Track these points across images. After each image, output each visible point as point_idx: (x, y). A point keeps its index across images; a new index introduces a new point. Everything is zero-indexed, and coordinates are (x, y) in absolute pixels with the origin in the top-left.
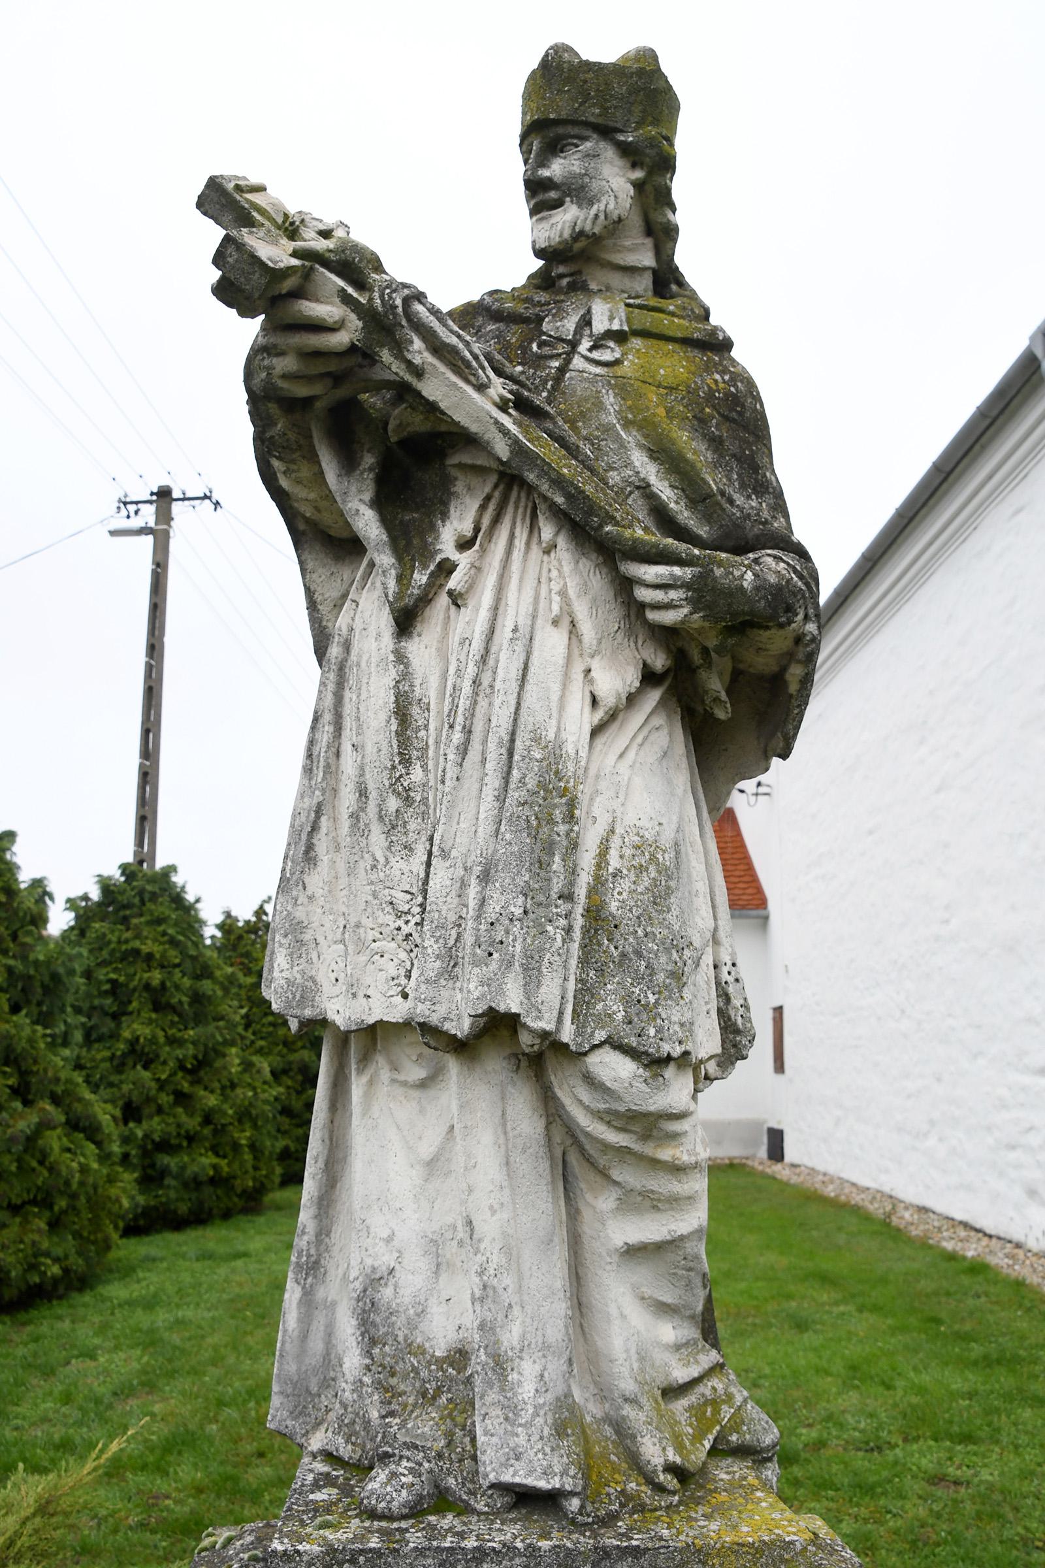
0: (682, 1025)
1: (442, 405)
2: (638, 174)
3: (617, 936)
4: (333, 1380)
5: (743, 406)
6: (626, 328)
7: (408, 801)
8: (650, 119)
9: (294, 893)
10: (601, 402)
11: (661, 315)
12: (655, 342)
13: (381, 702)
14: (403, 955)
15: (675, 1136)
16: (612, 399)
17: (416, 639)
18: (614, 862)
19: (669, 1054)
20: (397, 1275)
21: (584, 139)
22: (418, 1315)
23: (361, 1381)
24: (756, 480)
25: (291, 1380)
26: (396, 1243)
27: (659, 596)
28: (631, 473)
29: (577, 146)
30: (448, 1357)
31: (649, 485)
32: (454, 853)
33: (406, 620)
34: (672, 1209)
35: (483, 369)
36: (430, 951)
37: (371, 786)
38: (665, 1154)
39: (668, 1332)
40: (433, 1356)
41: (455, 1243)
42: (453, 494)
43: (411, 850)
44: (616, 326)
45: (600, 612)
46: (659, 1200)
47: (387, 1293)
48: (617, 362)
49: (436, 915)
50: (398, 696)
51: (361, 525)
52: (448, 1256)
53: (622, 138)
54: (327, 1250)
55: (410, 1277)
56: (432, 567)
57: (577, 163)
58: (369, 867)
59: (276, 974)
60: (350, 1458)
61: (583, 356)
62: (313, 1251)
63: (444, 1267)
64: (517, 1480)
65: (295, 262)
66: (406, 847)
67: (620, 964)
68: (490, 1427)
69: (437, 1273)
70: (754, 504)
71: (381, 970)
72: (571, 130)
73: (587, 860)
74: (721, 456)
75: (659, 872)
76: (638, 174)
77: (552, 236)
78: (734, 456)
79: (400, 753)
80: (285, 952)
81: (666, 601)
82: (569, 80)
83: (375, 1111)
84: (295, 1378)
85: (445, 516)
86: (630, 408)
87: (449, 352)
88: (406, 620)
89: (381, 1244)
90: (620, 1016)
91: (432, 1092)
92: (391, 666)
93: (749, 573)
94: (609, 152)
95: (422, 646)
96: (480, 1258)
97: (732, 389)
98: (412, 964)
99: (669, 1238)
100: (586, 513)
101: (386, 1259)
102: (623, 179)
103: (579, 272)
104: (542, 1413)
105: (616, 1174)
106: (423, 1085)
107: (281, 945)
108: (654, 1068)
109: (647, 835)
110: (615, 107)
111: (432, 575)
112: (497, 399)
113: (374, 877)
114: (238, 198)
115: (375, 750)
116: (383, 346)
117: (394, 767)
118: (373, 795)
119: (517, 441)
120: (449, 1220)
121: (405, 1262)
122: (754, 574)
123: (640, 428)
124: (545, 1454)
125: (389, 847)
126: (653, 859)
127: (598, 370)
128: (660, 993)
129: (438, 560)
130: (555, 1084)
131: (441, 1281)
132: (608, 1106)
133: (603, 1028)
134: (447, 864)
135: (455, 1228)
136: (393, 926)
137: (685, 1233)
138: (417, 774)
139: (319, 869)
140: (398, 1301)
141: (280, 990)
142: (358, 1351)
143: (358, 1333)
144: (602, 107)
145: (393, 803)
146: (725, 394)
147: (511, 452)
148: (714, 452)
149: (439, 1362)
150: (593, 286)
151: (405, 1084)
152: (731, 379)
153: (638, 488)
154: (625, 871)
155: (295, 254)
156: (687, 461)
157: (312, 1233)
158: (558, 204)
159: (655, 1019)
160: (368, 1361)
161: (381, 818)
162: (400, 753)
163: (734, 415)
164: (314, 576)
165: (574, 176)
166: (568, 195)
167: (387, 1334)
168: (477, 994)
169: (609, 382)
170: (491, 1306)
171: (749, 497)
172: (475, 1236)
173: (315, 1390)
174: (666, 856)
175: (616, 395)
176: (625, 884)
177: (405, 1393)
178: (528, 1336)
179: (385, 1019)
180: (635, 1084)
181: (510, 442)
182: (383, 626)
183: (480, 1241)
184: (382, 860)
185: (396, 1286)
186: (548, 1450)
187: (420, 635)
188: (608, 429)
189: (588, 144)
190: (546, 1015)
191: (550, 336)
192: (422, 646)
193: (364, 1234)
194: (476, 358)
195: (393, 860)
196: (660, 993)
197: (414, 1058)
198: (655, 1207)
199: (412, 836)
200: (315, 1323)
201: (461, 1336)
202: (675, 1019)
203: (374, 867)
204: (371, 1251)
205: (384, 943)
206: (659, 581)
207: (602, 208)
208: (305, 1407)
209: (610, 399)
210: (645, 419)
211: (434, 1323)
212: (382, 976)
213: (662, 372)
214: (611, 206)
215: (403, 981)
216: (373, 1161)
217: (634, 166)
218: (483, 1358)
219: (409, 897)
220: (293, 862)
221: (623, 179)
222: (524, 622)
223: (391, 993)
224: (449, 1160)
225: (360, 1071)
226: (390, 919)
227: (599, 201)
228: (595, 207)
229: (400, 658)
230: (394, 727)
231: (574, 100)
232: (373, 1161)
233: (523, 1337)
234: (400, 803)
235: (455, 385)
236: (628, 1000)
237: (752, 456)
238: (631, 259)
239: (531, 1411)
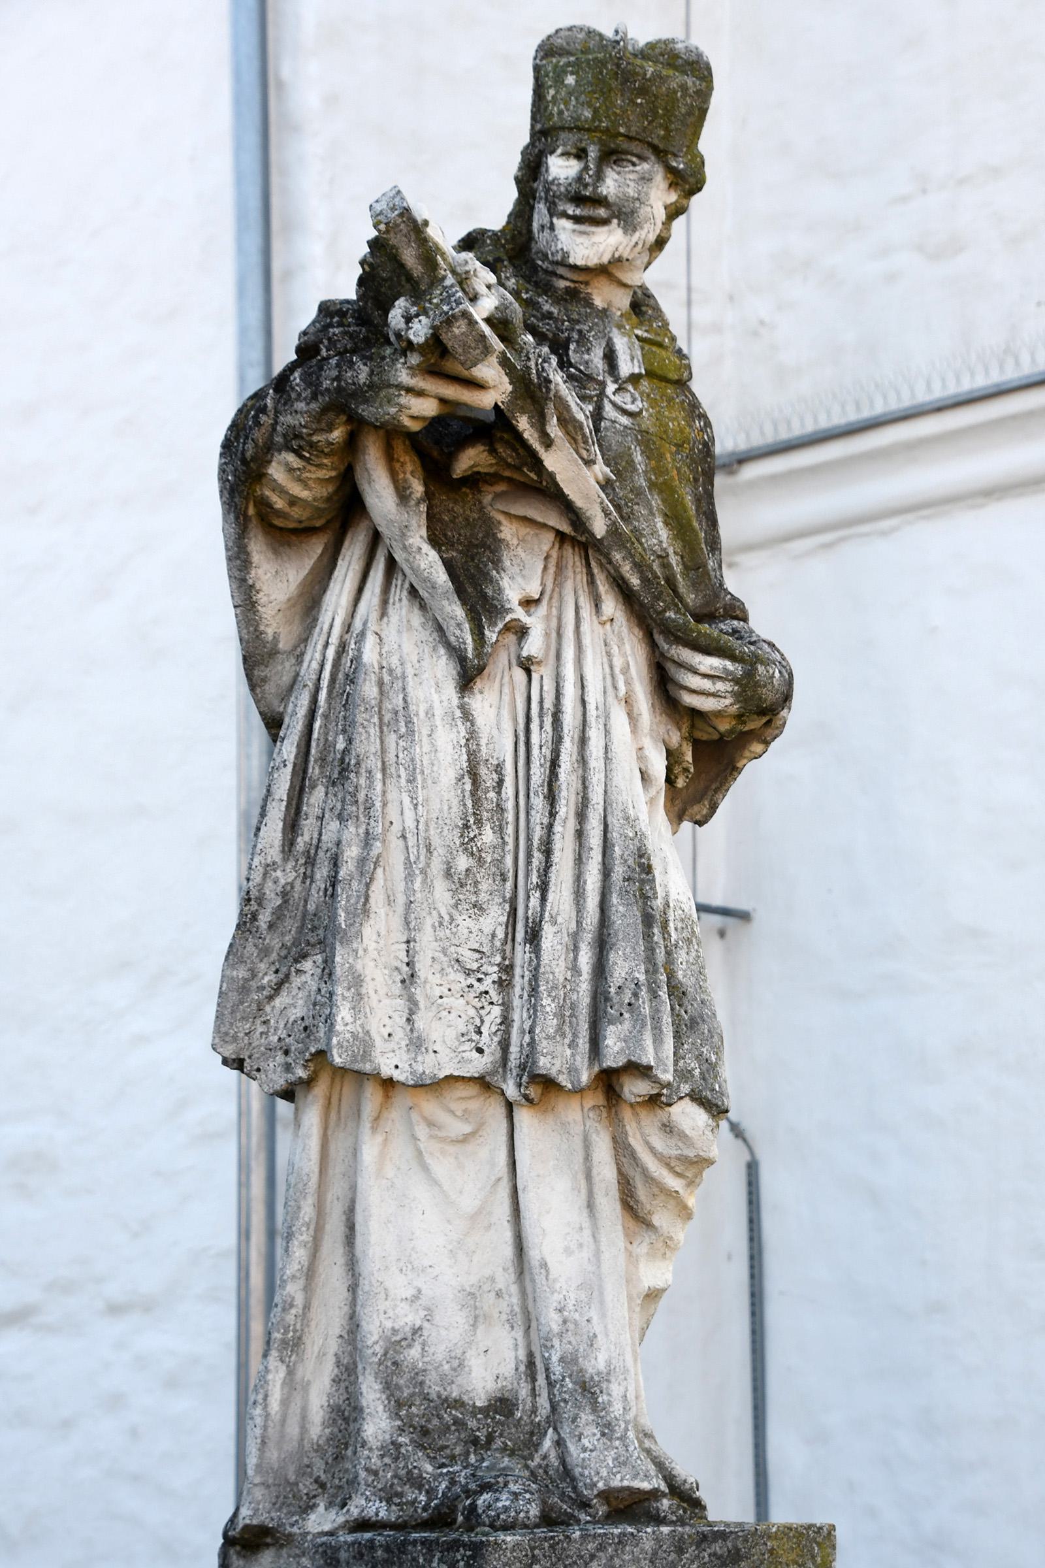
1: (558, 478)
3: (685, 1001)
4: (308, 1466)
7: (480, 861)
9: (355, 945)
10: (633, 461)
13: (449, 759)
14: (472, 1012)
16: (639, 457)
17: (479, 696)
20: (425, 1333)
21: (642, 158)
22: (455, 1370)
23: (397, 1445)
25: (272, 1469)
26: (423, 1301)
27: (706, 684)
28: (655, 541)
29: (634, 164)
30: (489, 1406)
32: (560, 920)
33: (468, 676)
36: (548, 1009)
37: (436, 841)
40: (474, 1406)
41: (493, 1294)
42: (501, 541)
43: (481, 909)
47: (414, 1353)
49: (551, 977)
50: (469, 754)
51: (423, 566)
52: (486, 1308)
53: (674, 164)
54: (308, 1326)
55: (443, 1332)
56: (500, 625)
57: (632, 184)
58: (437, 924)
59: (339, 1027)
60: (397, 1518)
62: (298, 1327)
63: (481, 1320)
64: (626, 1483)
66: (475, 906)
67: (691, 1028)
68: (587, 1444)
69: (474, 1326)
71: (449, 1026)
72: (635, 147)
77: (591, 256)
79: (474, 814)
80: (348, 1005)
81: (712, 690)
82: (643, 91)
83: (390, 1172)
84: (276, 1466)
85: (497, 563)
86: (653, 469)
87: (575, 427)
88: (468, 676)
89: (403, 1304)
91: (469, 1147)
92: (459, 723)
95: (486, 704)
96: (556, 1297)
98: (482, 1022)
100: (655, 597)
101: (408, 1317)
103: (587, 283)
105: (656, 1220)
106: (465, 1139)
107: (344, 998)
110: (677, 129)
111: (499, 633)
112: (601, 477)
113: (441, 934)
115: (446, 808)
116: (523, 413)
117: (466, 826)
118: (440, 852)
119: (614, 523)
120: (487, 1272)
121: (437, 1319)
123: (661, 492)
125: (456, 906)
127: (625, 420)
129: (507, 619)
130: (630, 1133)
131: (478, 1331)
132: (679, 1152)
133: (686, 1082)
134: (555, 929)
135: (492, 1279)
136: (464, 984)
138: (488, 836)
139: (372, 922)
140: (426, 1359)
141: (345, 1044)
142: (386, 1415)
143: (384, 1397)
144: (667, 129)
145: (463, 862)
147: (607, 532)
149: (481, 1410)
150: (599, 302)
151: (443, 1140)
153: (659, 557)
157: (301, 1306)
158: (604, 222)
160: (399, 1423)
161: (448, 874)
162: (474, 814)
164: (260, 572)
165: (628, 199)
166: (618, 217)
167: (413, 1395)
168: (616, 1049)
169: (637, 439)
170: (572, 1339)
172: (550, 1277)
173: (292, 1478)
175: (643, 452)
177: (447, 1447)
178: (613, 1361)
179: (456, 1074)
181: (609, 522)
182: (439, 675)
183: (555, 1280)
184: (447, 918)
185: (424, 1344)
187: (482, 693)
188: (638, 492)
189: (646, 166)
191: (580, 371)
192: (486, 704)
193: (382, 1295)
195: (459, 919)
197: (459, 1113)
199: (483, 897)
200: (293, 1404)
201: (499, 1385)
203: (441, 924)
204: (390, 1313)
205: (452, 999)
206: (712, 673)
207: (643, 237)
208: (285, 1497)
210: (665, 483)
211: (473, 1375)
212: (451, 1034)
215: (475, 1037)
216: (390, 1222)
218: (570, 1386)
219: (477, 955)
220: (347, 913)
222: (601, 699)
223: (462, 1048)
224: (490, 1213)
225: (374, 1129)
226: (461, 977)
227: (642, 228)
228: (637, 234)
229: (467, 716)
230: (468, 787)
231: (644, 116)
232: (390, 1222)
233: (609, 1363)
234: (471, 862)
236: (699, 1057)
239: (623, 1426)
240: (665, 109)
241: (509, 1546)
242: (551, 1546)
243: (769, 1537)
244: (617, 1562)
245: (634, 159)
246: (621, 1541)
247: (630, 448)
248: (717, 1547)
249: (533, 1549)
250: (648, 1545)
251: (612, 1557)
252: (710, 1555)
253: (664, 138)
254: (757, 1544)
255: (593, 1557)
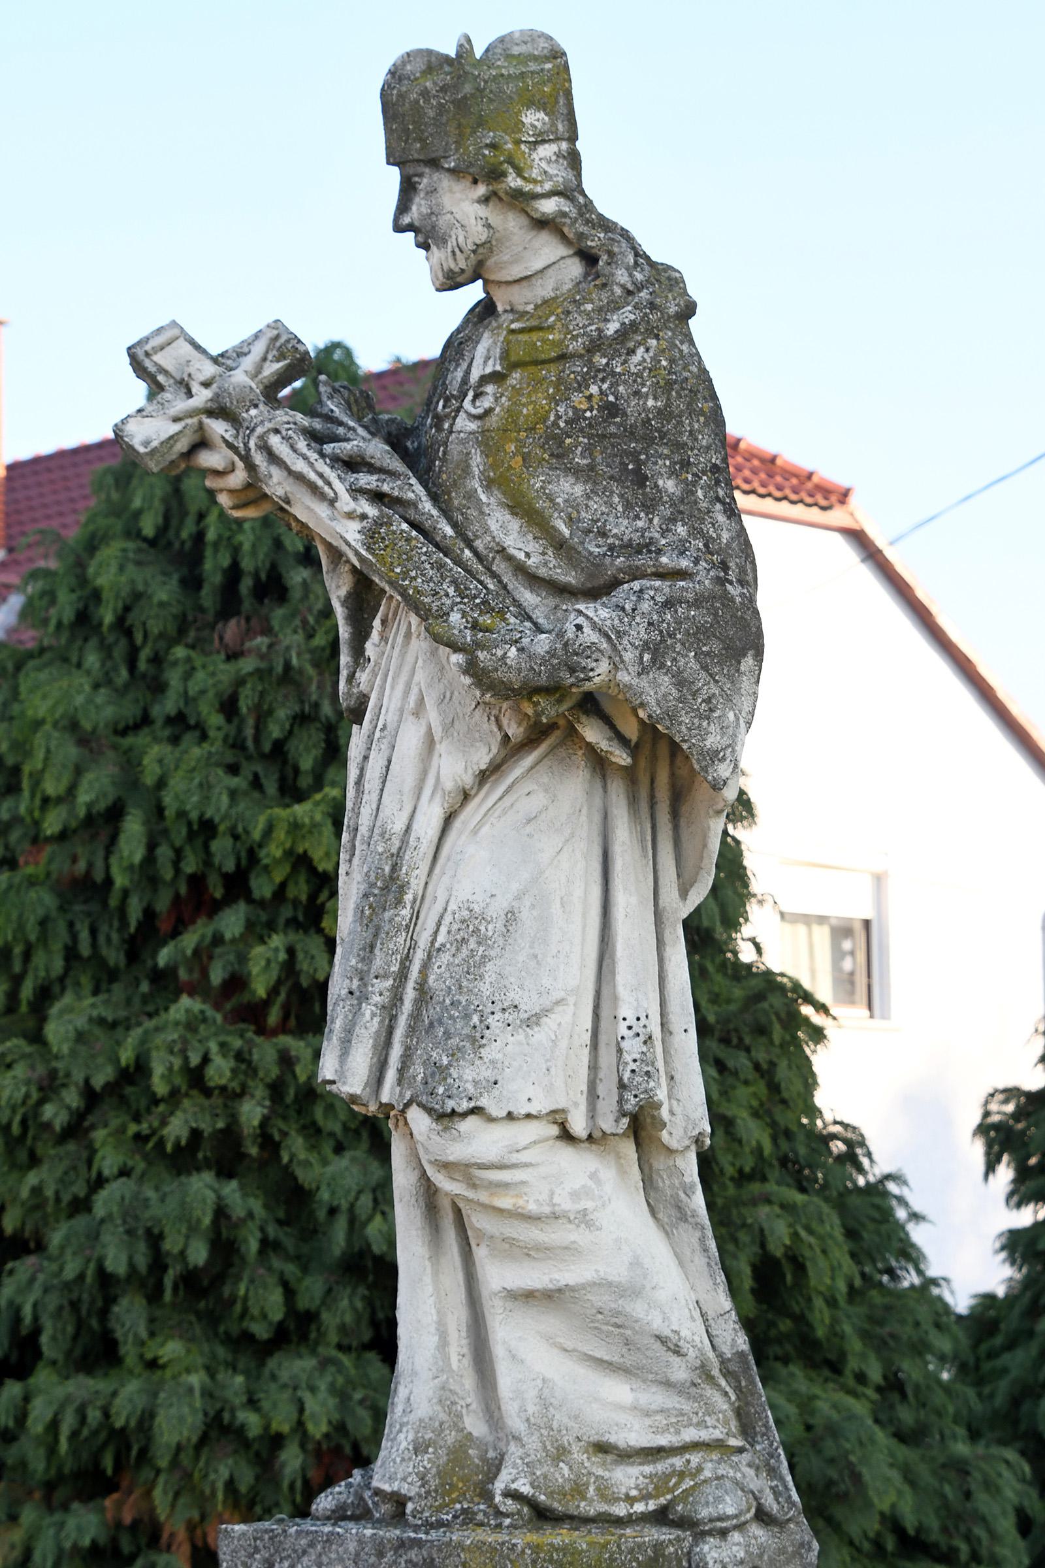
0: (476, 1083)
2: (481, 190)
5: (625, 414)
6: (498, 368)
8: (468, 130)
10: (469, 466)
11: (535, 336)
12: (532, 369)
15: (506, 1186)
16: (479, 459)
18: (441, 939)
19: (453, 1110)
21: (421, 175)
24: (644, 494)
28: (489, 539)
31: (504, 549)
34: (550, 1258)
35: (329, 484)
38: (505, 1202)
39: (619, 1391)
44: (488, 370)
45: (456, 693)
46: (529, 1249)
48: (488, 412)
53: (446, 166)
61: (466, 412)
65: (176, 428)
70: (640, 524)
73: (423, 940)
74: (595, 483)
75: (479, 943)
76: (481, 190)
78: (611, 478)
90: (419, 1078)
93: (513, 649)
94: (445, 182)
97: (611, 398)
99: (551, 1286)
102: (467, 203)
104: (405, 1430)
108: (446, 1121)
109: (477, 909)
110: (431, 135)
114: (148, 364)
122: (518, 650)
124: (395, 1463)
126: (476, 931)
127: (473, 426)
128: (453, 1055)
137: (571, 1283)
144: (422, 140)
146: (600, 408)
148: (586, 482)
152: (612, 385)
153: (498, 552)
154: (448, 946)
155: (176, 420)
156: (537, 512)
159: (445, 1079)
163: (613, 429)
171: (637, 517)
174: (490, 927)
176: (445, 958)
180: (432, 1136)
186: (398, 1460)
188: (471, 495)
189: (425, 181)
190: (350, 1080)
194: (321, 475)
196: (453, 1055)
198: (528, 1255)
202: (465, 1077)
207: (455, 244)
209: (477, 460)
213: (525, 411)
214: (461, 240)
217: (475, 182)
221: (467, 203)
235: (308, 508)
237: (637, 471)
238: (516, 272)
240: (414, 122)
241: (236, 1535)
242: (271, 1538)
243: (463, 1550)
244: (325, 1559)
245: (416, 179)
246: (329, 1540)
247: (468, 454)
248: (413, 1554)
249: (255, 1539)
250: (352, 1546)
251: (320, 1555)
252: (406, 1562)
253: (422, 149)
254: (450, 1555)
255: (304, 1552)
